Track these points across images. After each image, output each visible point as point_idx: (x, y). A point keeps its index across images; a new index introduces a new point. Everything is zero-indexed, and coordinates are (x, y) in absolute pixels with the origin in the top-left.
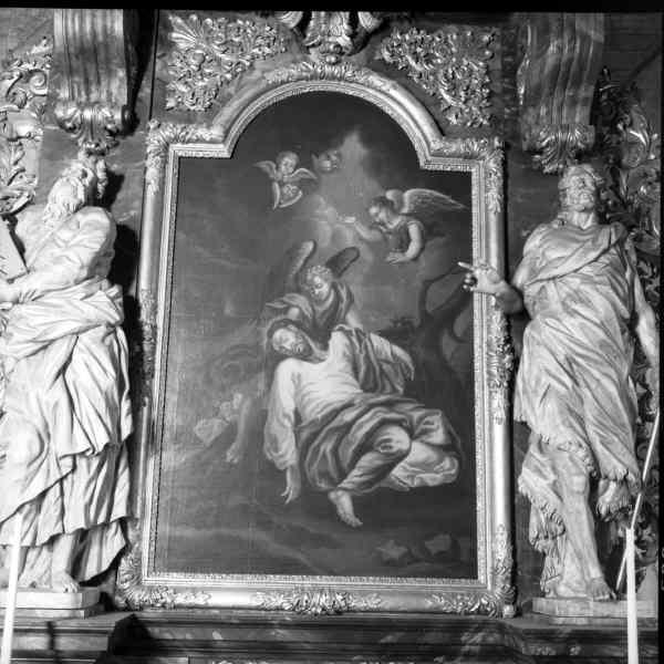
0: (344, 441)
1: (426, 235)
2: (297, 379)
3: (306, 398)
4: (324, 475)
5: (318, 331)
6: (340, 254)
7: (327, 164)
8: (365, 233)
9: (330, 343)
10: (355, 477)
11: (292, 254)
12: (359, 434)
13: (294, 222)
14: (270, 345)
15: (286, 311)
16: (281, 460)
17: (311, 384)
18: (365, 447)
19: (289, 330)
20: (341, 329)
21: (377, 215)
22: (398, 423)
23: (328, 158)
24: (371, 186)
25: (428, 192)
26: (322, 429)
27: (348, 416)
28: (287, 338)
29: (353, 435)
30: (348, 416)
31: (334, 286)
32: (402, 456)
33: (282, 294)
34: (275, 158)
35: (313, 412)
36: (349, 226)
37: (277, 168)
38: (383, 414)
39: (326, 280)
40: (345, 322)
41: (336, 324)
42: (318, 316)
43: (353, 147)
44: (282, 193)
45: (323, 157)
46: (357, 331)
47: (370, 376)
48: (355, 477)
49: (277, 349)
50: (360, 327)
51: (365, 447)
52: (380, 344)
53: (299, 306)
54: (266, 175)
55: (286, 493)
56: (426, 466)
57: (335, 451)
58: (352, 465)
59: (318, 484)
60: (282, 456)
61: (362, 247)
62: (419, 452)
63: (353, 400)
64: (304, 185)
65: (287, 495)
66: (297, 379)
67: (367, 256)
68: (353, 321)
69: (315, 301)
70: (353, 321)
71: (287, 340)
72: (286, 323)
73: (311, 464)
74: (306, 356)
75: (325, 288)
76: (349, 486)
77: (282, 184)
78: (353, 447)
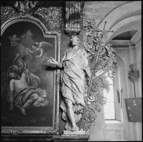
0: (24, 97)
2: (14, 84)
3: (16, 88)
4: (19, 104)
6: (25, 56)
7: (23, 37)
9: (22, 76)
10: (26, 105)
11: (14, 56)
12: (27, 95)
14: (9, 76)
15: (12, 69)
16: (10, 101)
17: (17, 84)
18: (29, 98)
19: (13, 73)
20: (24, 72)
21: (33, 48)
22: (36, 93)
23: (23, 36)
25: (45, 42)
26: (19, 94)
27: (25, 91)
29: (26, 96)
30: (25, 91)
31: (23, 63)
32: (36, 100)
33: (12, 65)
36: (27, 50)
37: (12, 38)
39: (21, 62)
40: (25, 71)
41: (23, 72)
42: (19, 70)
43: (29, 33)
44: (13, 43)
45: (22, 35)
46: (28, 73)
48: (26, 105)
49: (10, 77)
50: (29, 72)
51: (29, 98)
52: (32, 75)
54: (10, 39)
55: (10, 109)
56: (42, 102)
57: (22, 99)
58: (25, 102)
59: (18, 106)
60: (10, 100)
61: (30, 54)
63: (26, 88)
65: (11, 109)
66: (14, 84)
68: (27, 71)
69: (19, 66)
71: (12, 75)
72: (12, 72)
73: (16, 102)
74: (16, 78)
75: (21, 64)
76: (25, 107)
77: (13, 41)
78: (26, 98)
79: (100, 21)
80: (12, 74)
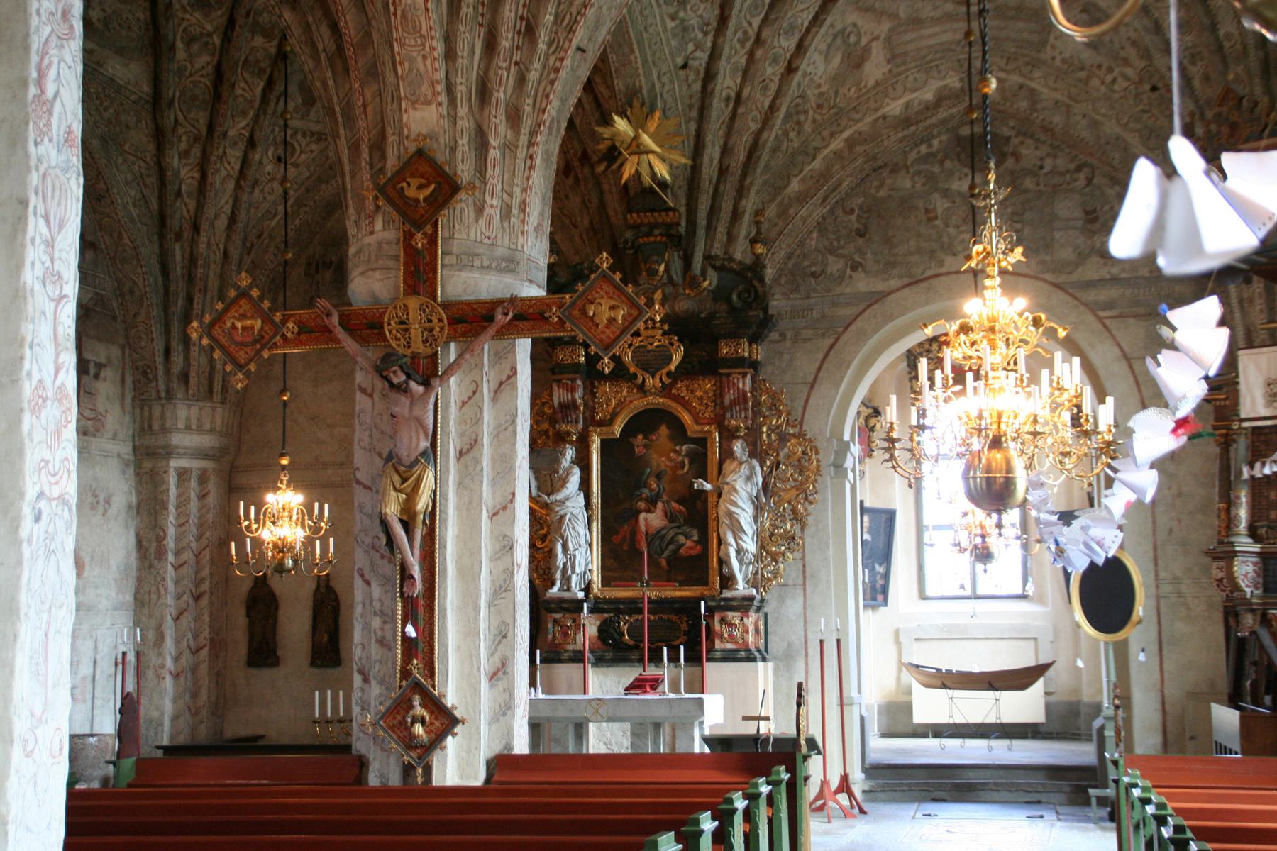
1: (691, 463)
2: (646, 520)
5: (652, 503)
8: (668, 463)
10: (666, 553)
11: (643, 473)
12: (668, 538)
13: (642, 462)
18: (670, 543)
24: (669, 445)
28: (642, 505)
32: (683, 545)
34: (635, 437)
35: (651, 531)
38: (676, 530)
43: (664, 430)
47: (670, 516)
48: (666, 553)
51: (670, 543)
52: (674, 504)
53: (646, 492)
56: (691, 548)
62: (689, 543)
64: (646, 446)
66: (646, 520)
67: (669, 472)
68: (665, 498)
69: (651, 490)
70: (665, 498)
72: (641, 500)
74: (649, 511)
79: (832, 341)
80: (642, 505)
